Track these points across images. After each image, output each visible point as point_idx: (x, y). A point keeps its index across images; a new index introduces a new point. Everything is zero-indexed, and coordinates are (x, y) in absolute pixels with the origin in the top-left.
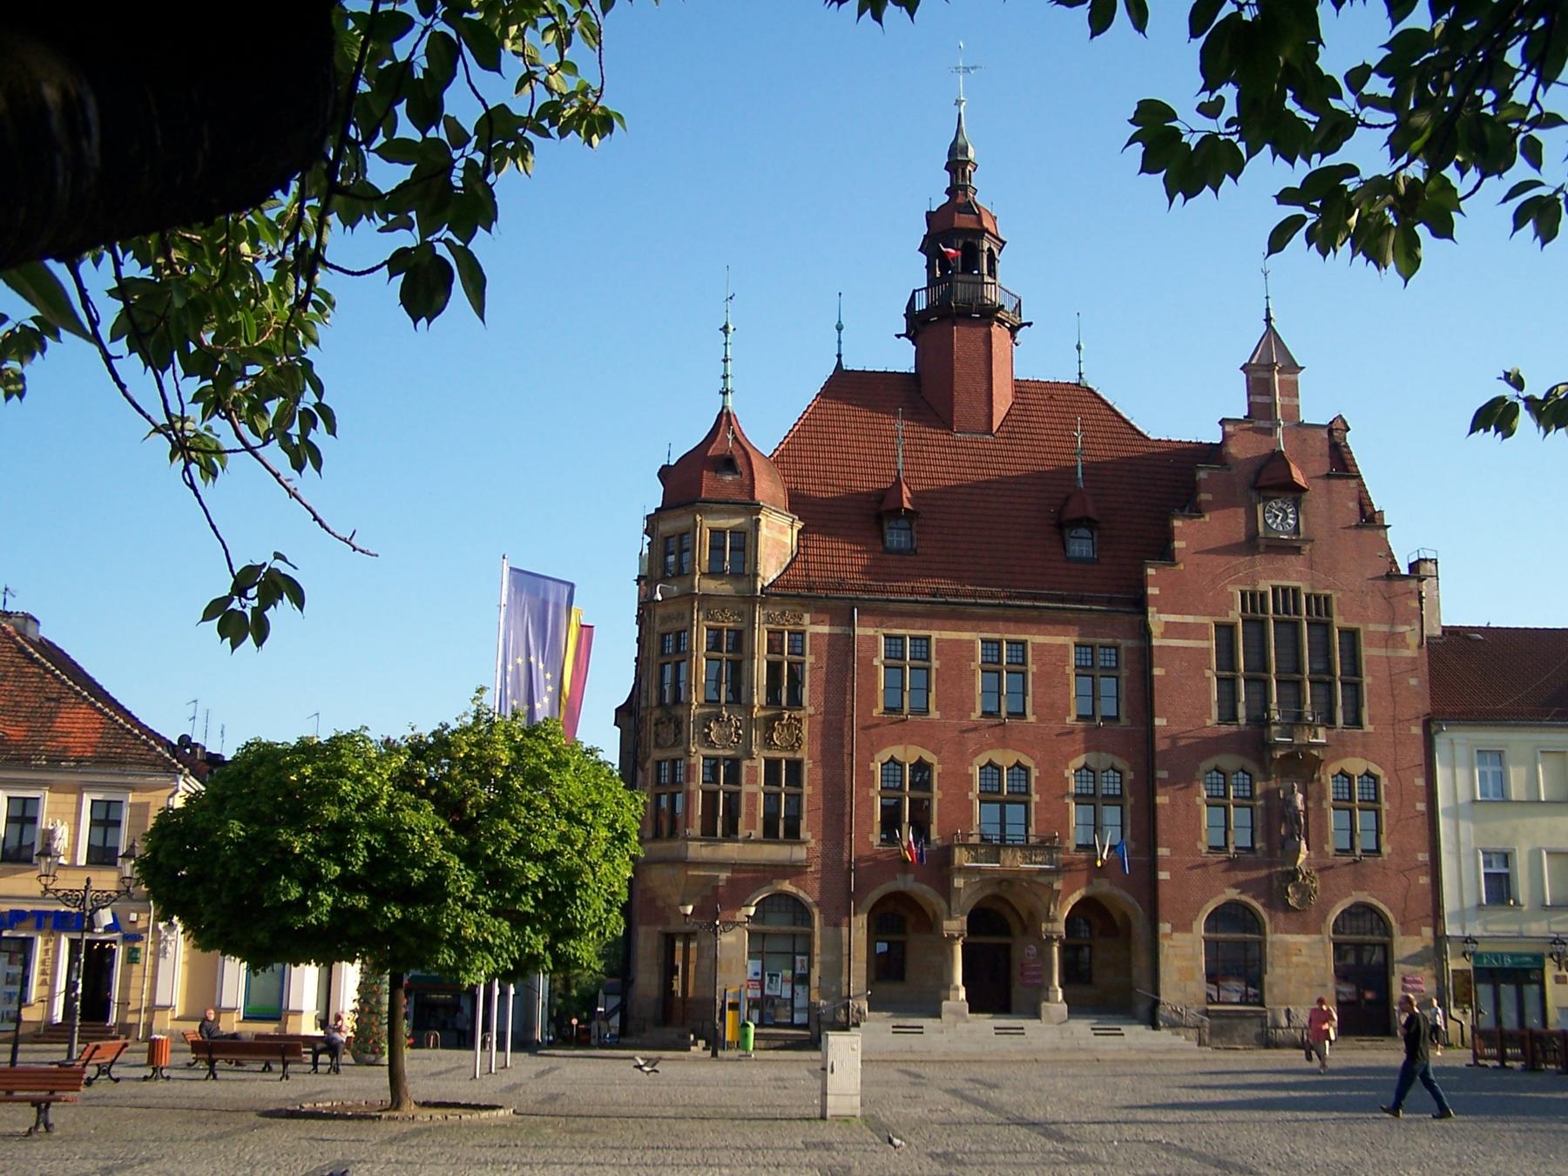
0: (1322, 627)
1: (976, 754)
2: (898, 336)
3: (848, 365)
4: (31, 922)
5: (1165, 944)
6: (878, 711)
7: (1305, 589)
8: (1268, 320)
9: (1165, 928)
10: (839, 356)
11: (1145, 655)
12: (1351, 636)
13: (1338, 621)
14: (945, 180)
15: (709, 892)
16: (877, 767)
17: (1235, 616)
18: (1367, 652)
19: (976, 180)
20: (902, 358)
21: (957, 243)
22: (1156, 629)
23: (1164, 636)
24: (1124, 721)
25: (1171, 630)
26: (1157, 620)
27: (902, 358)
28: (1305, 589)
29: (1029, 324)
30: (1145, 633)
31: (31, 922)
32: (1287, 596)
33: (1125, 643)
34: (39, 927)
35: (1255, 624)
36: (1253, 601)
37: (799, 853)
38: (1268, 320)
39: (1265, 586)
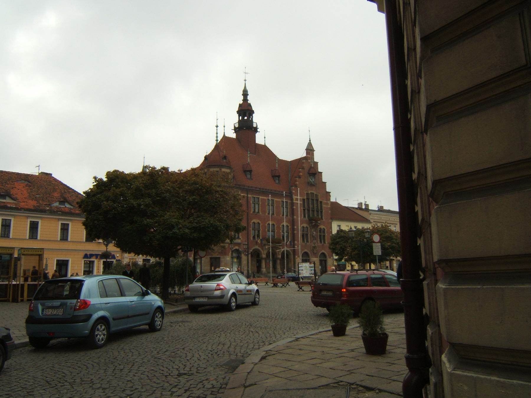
0: (317, 200)
3: (227, 135)
4: (94, 257)
6: (252, 212)
7: (315, 193)
9: (296, 257)
12: (321, 202)
13: (320, 200)
14: (242, 98)
17: (305, 197)
18: (324, 206)
19: (249, 97)
20: (234, 136)
21: (245, 110)
22: (294, 199)
27: (234, 136)
28: (315, 193)
31: (94, 257)
32: (312, 194)
33: (289, 201)
34: (97, 258)
35: (308, 199)
36: (307, 194)
38: (310, 141)
39: (309, 192)
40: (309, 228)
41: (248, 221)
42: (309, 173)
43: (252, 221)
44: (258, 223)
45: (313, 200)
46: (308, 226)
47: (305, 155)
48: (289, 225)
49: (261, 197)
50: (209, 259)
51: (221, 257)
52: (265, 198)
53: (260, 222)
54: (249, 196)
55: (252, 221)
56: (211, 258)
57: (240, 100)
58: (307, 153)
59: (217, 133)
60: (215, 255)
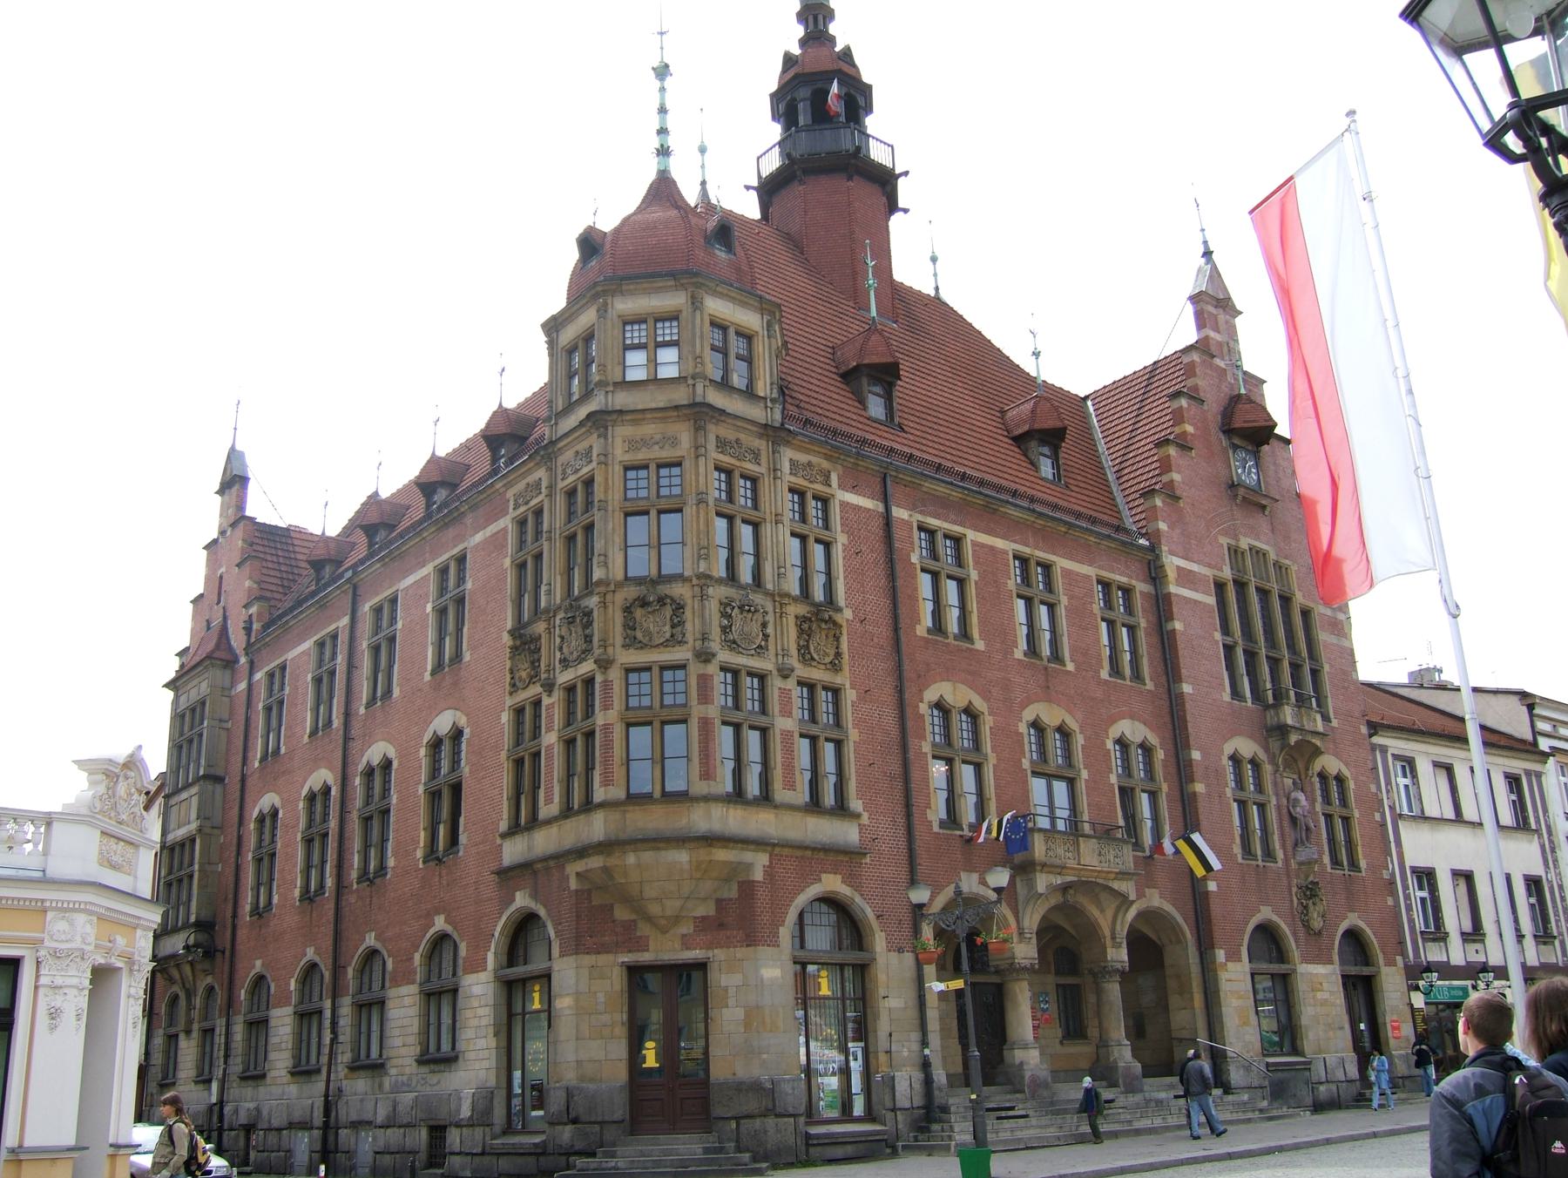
0: (1286, 600)
1: (1023, 706)
2: (748, 188)
5: (1223, 976)
6: (921, 631)
8: (1208, 254)
9: (1220, 955)
10: (703, 183)
11: (1162, 606)
12: (1306, 614)
13: (1299, 598)
15: (732, 892)
16: (923, 708)
17: (1227, 573)
22: (1171, 574)
23: (1179, 583)
24: (1150, 685)
25: (1185, 577)
26: (1172, 563)
29: (906, 211)
30: (1155, 574)
37: (847, 833)
38: (1208, 254)
39: (1244, 543)
40: (1268, 768)
41: (900, 691)
42: (1228, 431)
43: (931, 695)
44: (969, 711)
45: (1264, 593)
46: (1262, 755)
47: (1188, 334)
48: (1153, 740)
49: (971, 535)
50: (616, 981)
51: (719, 954)
52: (999, 543)
53: (980, 704)
54: (899, 513)
55: (931, 695)
56: (635, 973)
57: (791, 36)
58: (1201, 320)
59: (663, 110)
60: (666, 949)
